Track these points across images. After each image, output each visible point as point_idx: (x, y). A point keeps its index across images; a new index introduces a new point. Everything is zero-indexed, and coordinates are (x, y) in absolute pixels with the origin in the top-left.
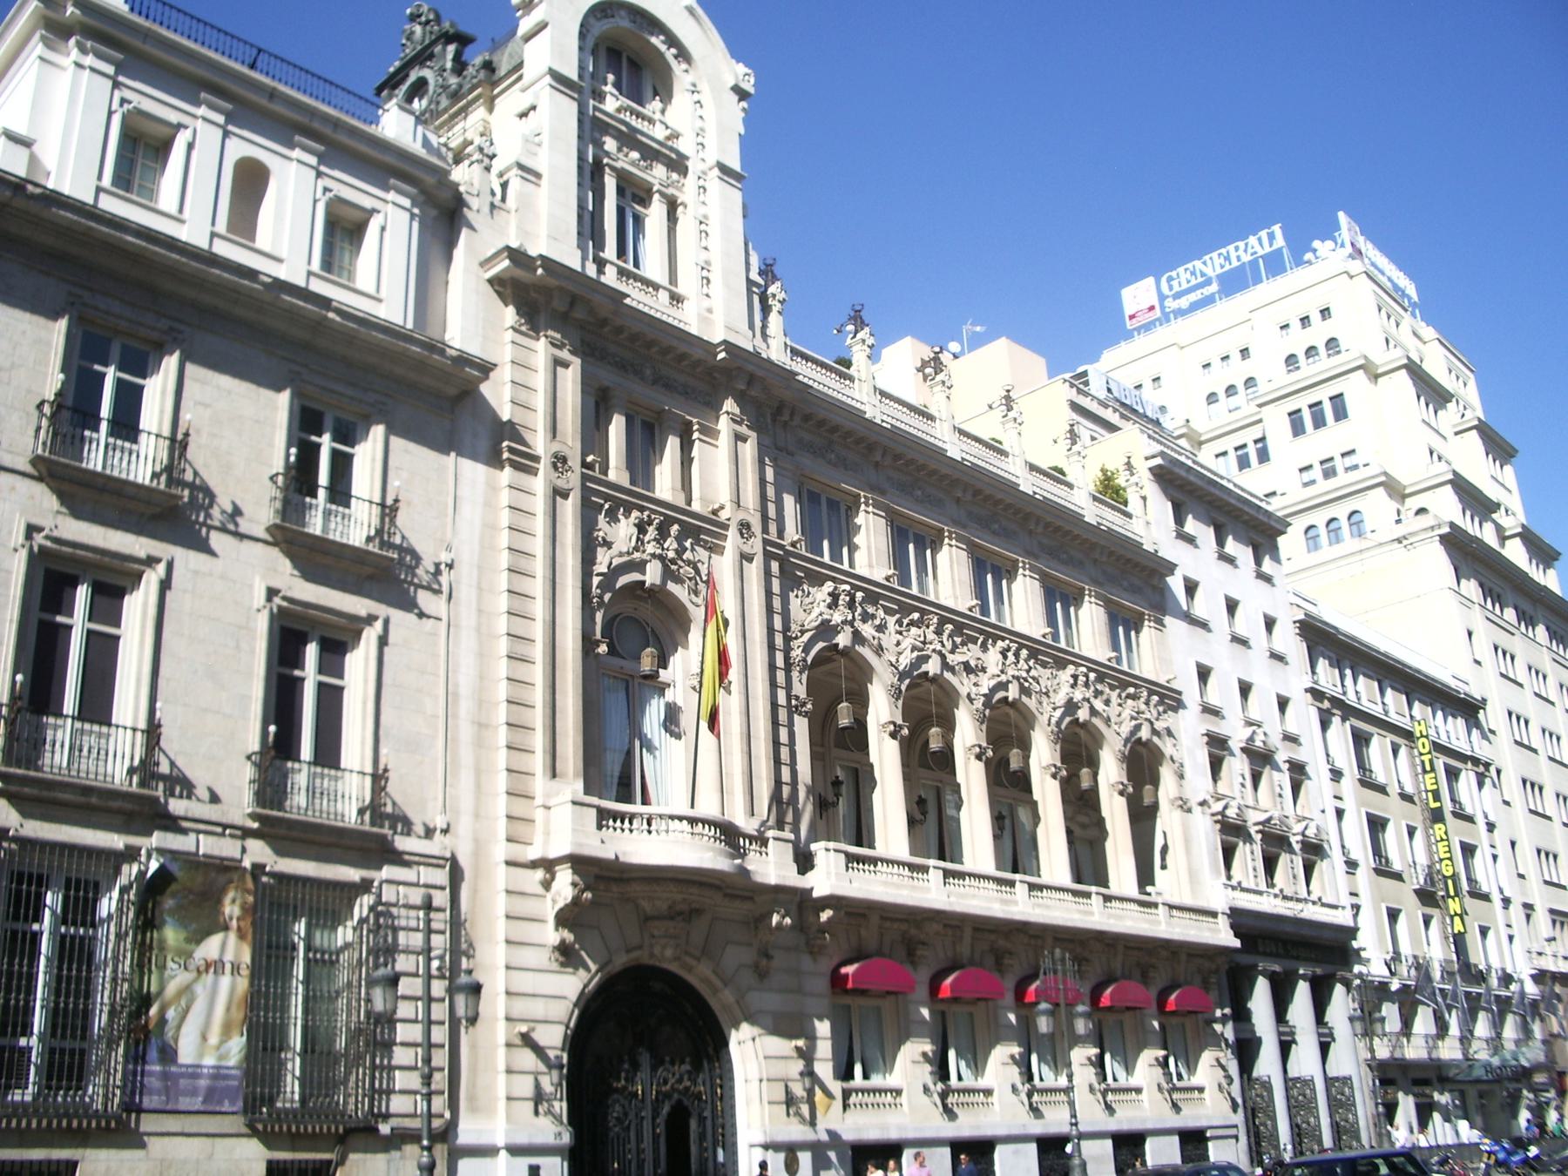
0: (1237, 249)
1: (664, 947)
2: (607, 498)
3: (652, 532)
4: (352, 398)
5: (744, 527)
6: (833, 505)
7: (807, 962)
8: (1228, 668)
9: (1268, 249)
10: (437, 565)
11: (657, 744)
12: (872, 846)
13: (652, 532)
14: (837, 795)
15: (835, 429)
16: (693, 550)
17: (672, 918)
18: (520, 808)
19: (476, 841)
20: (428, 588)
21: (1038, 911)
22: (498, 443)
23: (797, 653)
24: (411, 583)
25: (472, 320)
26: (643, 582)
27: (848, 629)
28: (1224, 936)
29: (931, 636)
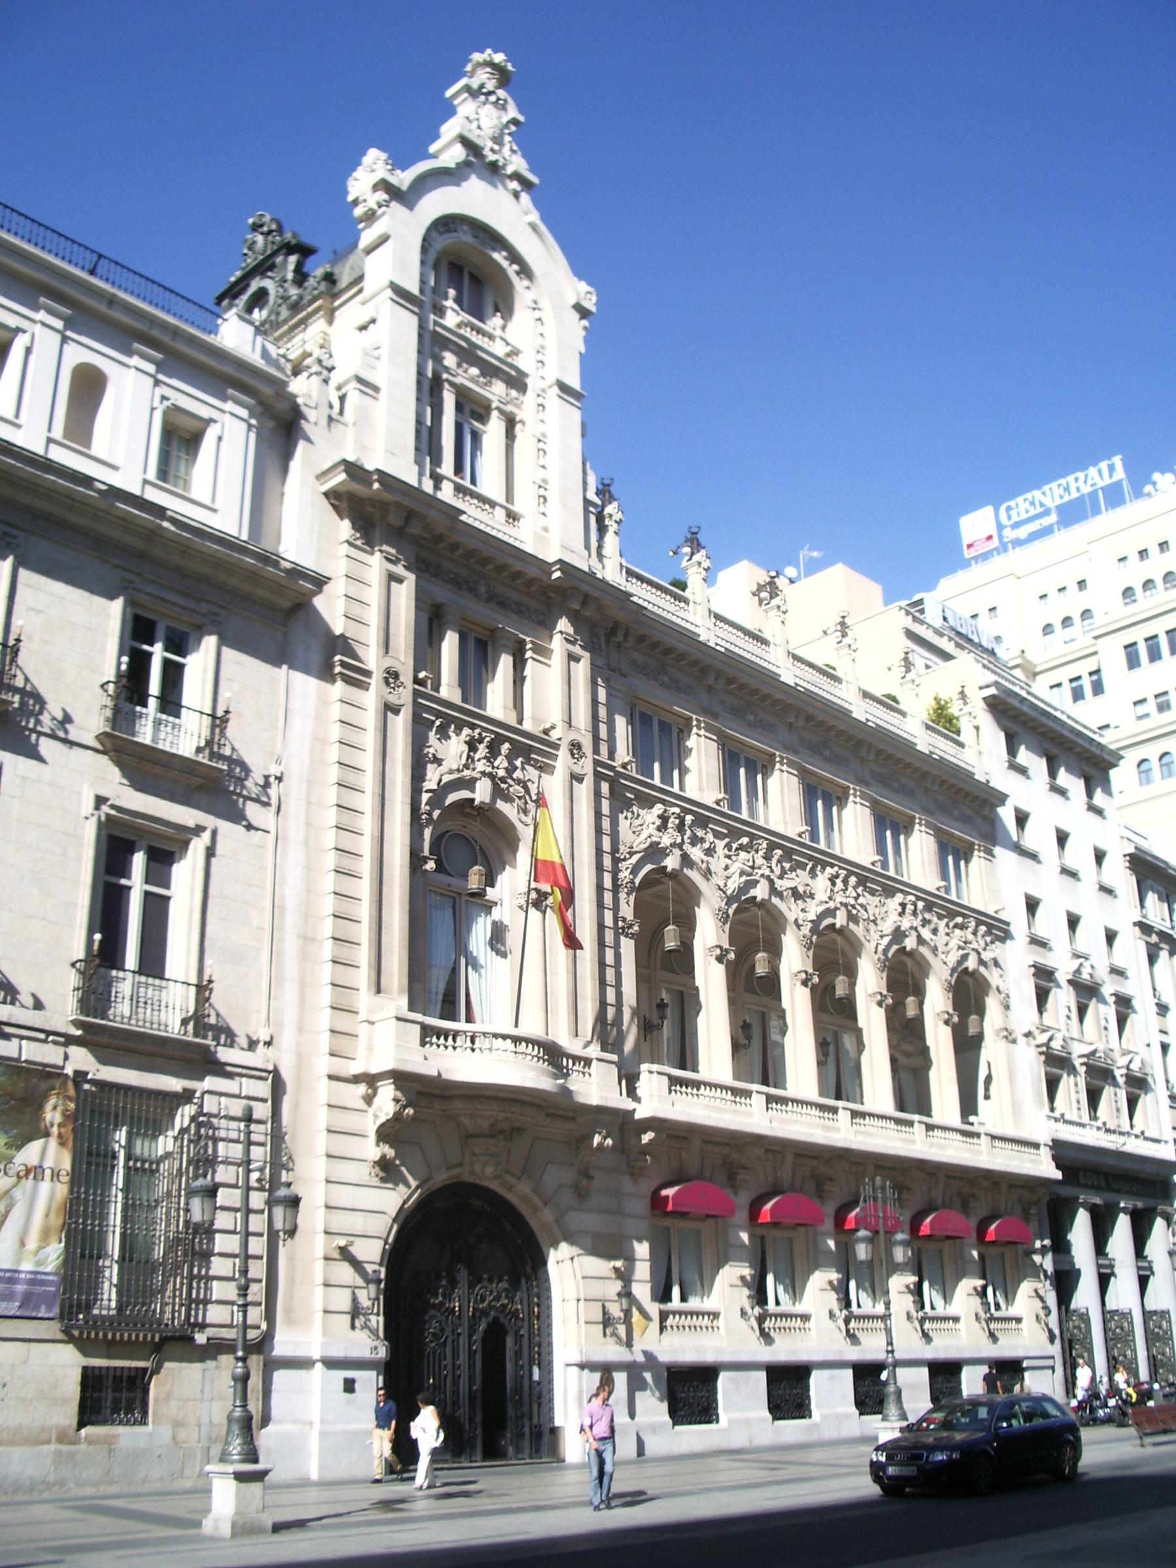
0: (1076, 479)
1: (484, 1165)
2: (439, 714)
3: (482, 750)
4: (185, 608)
5: (575, 748)
6: (665, 727)
7: (627, 1184)
8: (1057, 901)
9: (1107, 481)
10: (267, 777)
11: (482, 961)
12: (695, 1069)
13: (482, 750)
14: (662, 1018)
15: (668, 651)
16: (523, 769)
17: (493, 1136)
18: (344, 1022)
20: (257, 800)
21: (860, 1138)
22: (331, 657)
23: (624, 875)
24: (240, 795)
25: (308, 533)
26: (473, 800)
27: (677, 852)
28: (1045, 1167)
29: (760, 861)
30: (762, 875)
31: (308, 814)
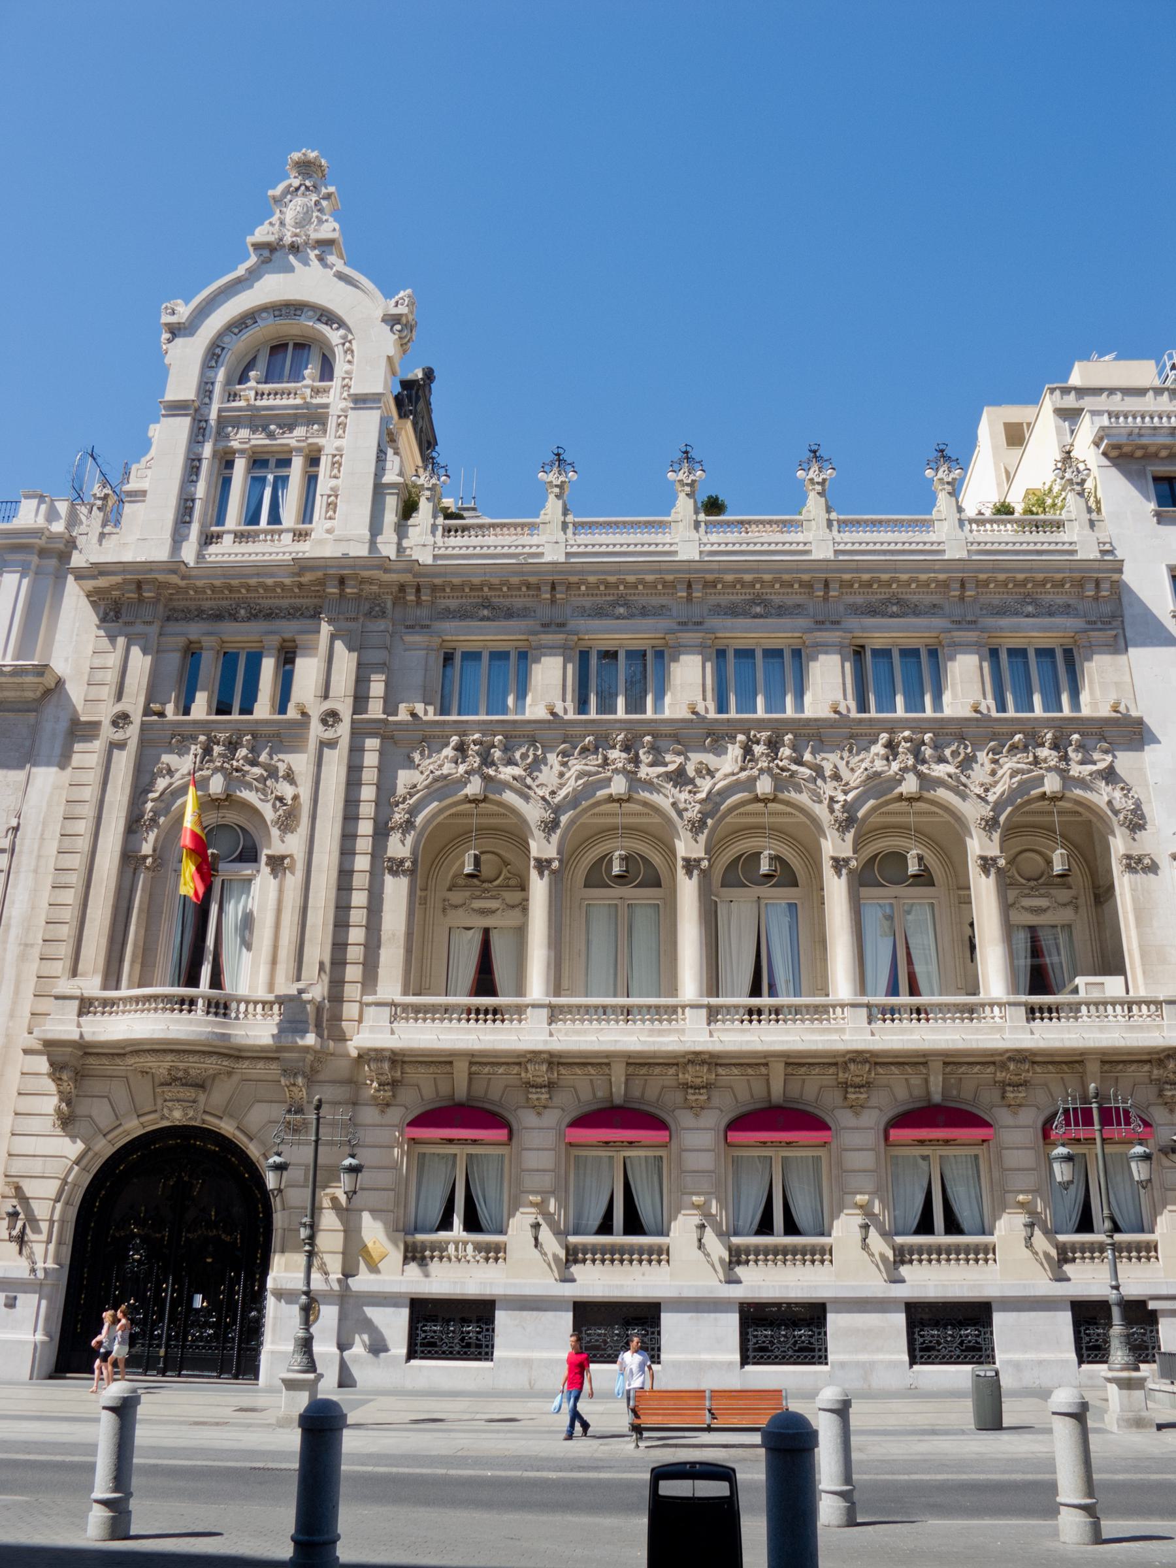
19: (7, 1035)
23: (399, 817)
30: (616, 771)
31: (39, 850)
